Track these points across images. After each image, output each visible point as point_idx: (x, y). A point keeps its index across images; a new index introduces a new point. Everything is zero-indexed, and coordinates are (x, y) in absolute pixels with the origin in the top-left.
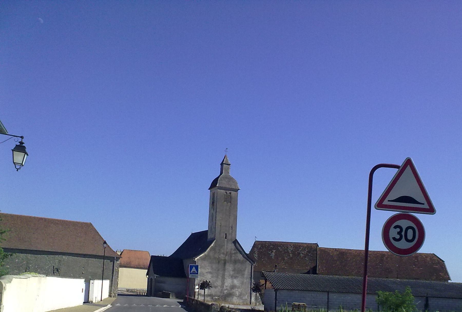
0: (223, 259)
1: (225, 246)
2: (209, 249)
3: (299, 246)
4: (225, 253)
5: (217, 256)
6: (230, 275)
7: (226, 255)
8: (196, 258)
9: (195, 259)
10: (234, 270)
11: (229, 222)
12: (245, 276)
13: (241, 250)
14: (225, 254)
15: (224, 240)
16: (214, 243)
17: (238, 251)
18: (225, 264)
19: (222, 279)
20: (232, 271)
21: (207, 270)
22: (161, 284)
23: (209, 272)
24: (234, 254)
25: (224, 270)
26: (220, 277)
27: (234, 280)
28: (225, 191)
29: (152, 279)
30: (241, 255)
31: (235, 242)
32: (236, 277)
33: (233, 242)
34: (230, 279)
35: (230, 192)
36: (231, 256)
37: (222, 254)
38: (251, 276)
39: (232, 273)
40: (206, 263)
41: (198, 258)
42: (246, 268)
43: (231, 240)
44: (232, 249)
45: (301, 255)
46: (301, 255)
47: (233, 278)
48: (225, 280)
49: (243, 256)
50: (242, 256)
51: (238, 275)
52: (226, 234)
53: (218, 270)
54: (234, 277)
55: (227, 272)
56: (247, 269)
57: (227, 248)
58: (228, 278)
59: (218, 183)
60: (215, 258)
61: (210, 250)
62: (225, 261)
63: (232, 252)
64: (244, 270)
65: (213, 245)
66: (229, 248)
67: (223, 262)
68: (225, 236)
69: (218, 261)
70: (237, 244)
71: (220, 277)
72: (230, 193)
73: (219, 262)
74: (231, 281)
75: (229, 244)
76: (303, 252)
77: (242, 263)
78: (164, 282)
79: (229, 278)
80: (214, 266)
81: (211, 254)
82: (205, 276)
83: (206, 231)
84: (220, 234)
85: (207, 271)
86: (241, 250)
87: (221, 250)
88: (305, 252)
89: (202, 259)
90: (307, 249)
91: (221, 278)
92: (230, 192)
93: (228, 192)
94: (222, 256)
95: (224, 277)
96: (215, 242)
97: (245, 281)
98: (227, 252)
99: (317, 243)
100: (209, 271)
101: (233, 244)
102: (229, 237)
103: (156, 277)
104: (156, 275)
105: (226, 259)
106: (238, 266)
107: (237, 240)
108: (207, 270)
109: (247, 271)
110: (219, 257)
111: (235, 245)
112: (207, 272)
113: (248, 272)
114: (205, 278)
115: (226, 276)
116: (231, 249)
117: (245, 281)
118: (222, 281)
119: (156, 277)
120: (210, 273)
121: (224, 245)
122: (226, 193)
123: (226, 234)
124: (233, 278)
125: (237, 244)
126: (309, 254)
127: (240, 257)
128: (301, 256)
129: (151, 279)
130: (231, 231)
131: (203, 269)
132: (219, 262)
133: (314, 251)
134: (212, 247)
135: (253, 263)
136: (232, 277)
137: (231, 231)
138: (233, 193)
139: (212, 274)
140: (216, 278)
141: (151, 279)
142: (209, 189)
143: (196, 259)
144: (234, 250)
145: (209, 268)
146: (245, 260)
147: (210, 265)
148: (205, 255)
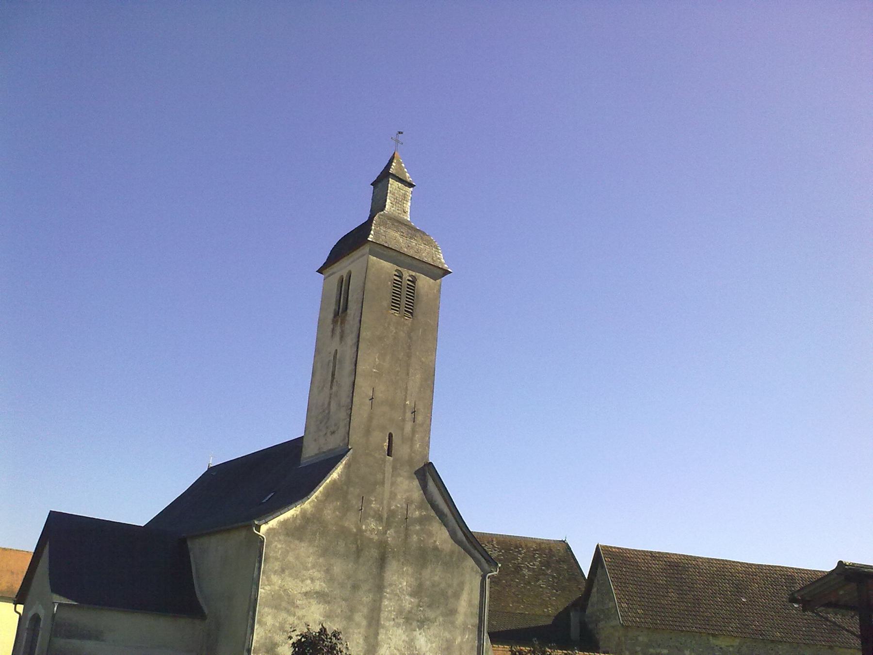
0: (376, 538)
1: (387, 485)
2: (321, 489)
3: (516, 547)
4: (385, 516)
5: (350, 523)
6: (400, 612)
7: (388, 526)
8: (266, 523)
9: (258, 528)
10: (417, 592)
11: (406, 389)
12: (460, 619)
13: (446, 510)
14: (385, 520)
15: (384, 461)
16: (345, 468)
17: (433, 513)
18: (382, 562)
19: (369, 625)
20: (411, 595)
21: (309, 582)
22: (76, 642)
23: (317, 593)
24: (422, 520)
25: (379, 588)
26: (359, 617)
27: (415, 633)
28: (396, 267)
29: (38, 616)
30: (443, 528)
31: (425, 476)
32: (423, 623)
33: (415, 473)
34: (400, 631)
35: (414, 274)
36: (406, 529)
37: (373, 517)
38: (481, 620)
39: (408, 602)
40: (306, 552)
41: (273, 523)
42: (461, 585)
43: (410, 462)
44: (412, 502)
45: (525, 571)
46: (525, 571)
47: (415, 624)
48: (382, 631)
49: (453, 535)
50: (448, 534)
51: (431, 614)
52: (390, 436)
53: (355, 587)
54: (418, 621)
55: (390, 599)
56: (467, 588)
57: (393, 496)
58: (392, 623)
59: (372, 232)
60: (343, 532)
61: (327, 494)
62: (385, 548)
63: (410, 515)
64: (457, 595)
65: (340, 476)
66: (399, 497)
67: (375, 553)
68: (386, 444)
69: (353, 548)
70: (431, 485)
71: (359, 617)
72: (414, 280)
73: (359, 552)
74: (404, 637)
75: (399, 479)
76: (529, 563)
77: (450, 563)
78: (95, 635)
79: (398, 625)
80: (338, 568)
81: (329, 514)
82: (297, 610)
83: (301, 439)
84: (368, 432)
85: (308, 589)
86: (446, 510)
87: (371, 502)
88: (534, 565)
89: (294, 531)
90: (538, 557)
91: (364, 623)
92: (414, 274)
93: (407, 274)
94: (372, 526)
95: (378, 621)
96: (348, 466)
97: (458, 640)
98: (392, 514)
99: (564, 540)
100: (318, 588)
101: (416, 483)
102: (402, 450)
103: (60, 605)
104: (58, 599)
105: (386, 542)
106: (434, 575)
107: (434, 464)
108: (308, 586)
109: (465, 596)
110: (360, 530)
111: (424, 487)
112: (306, 594)
113: (470, 602)
114: (299, 618)
115: (384, 615)
116: (409, 502)
117: (458, 640)
118: (366, 638)
119: (60, 605)
120: (321, 596)
121: (383, 483)
122: (401, 277)
123: (390, 436)
124: (411, 624)
125: (431, 485)
126: (548, 570)
127: (441, 536)
128: (524, 575)
129: (36, 619)
130: (408, 427)
131: (290, 575)
132: (359, 552)
133: (558, 562)
134: (334, 482)
135: (486, 566)
136: (408, 620)
137: (408, 427)
138: (424, 282)
139: (329, 603)
140: (345, 622)
141: (36, 619)
142: (372, 184)
143: (264, 528)
144: (420, 507)
145: (317, 574)
146: (459, 552)
147: (321, 560)
148: (304, 513)
